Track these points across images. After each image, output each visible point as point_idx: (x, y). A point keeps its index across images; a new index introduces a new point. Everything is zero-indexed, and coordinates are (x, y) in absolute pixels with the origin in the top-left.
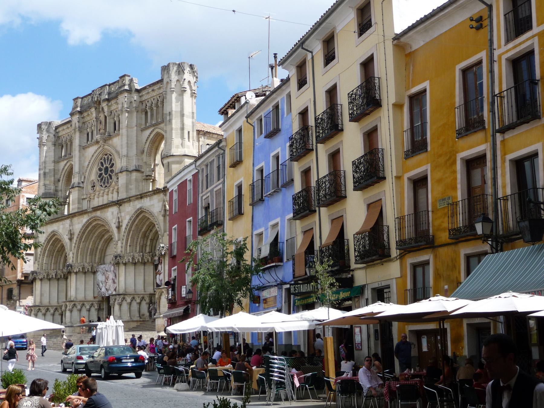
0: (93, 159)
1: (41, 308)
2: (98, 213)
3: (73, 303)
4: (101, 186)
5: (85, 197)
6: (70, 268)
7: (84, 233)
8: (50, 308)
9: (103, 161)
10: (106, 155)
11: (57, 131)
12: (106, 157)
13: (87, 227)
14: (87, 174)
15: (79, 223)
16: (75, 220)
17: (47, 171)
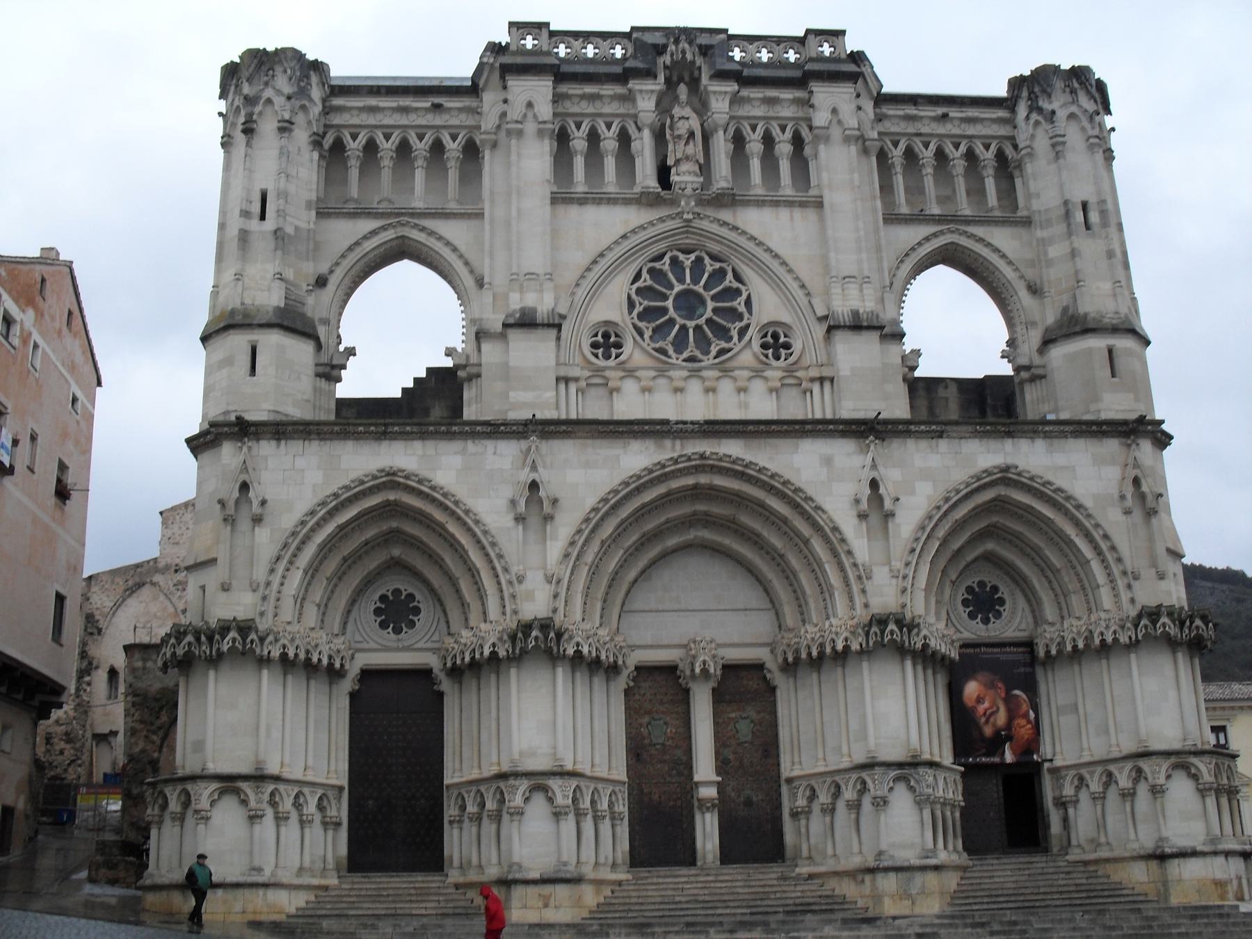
0: (619, 251)
1: (282, 787)
2: (733, 448)
3: (574, 783)
4: (662, 351)
5: (575, 372)
6: (552, 635)
7: (615, 507)
8: (306, 790)
9: (665, 265)
10: (687, 252)
11: (338, 101)
12: (688, 261)
13: (638, 490)
14: (581, 293)
15: (587, 465)
16: (563, 451)
17: (290, 230)
